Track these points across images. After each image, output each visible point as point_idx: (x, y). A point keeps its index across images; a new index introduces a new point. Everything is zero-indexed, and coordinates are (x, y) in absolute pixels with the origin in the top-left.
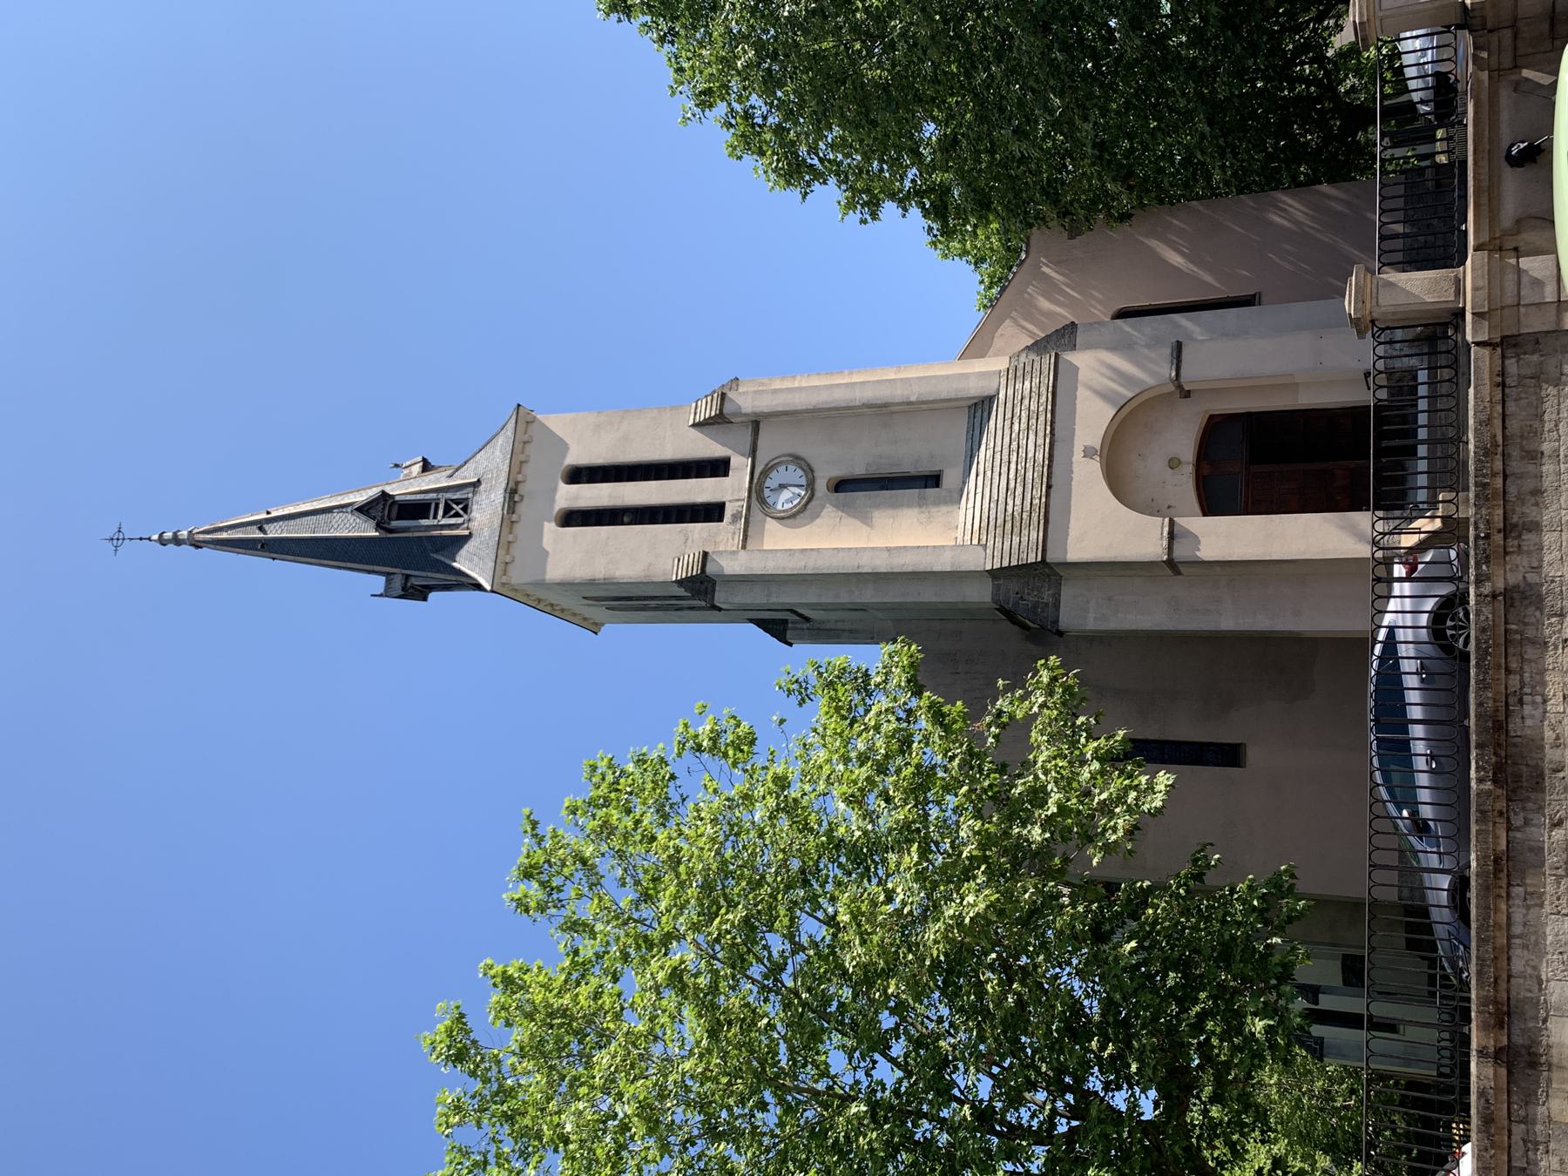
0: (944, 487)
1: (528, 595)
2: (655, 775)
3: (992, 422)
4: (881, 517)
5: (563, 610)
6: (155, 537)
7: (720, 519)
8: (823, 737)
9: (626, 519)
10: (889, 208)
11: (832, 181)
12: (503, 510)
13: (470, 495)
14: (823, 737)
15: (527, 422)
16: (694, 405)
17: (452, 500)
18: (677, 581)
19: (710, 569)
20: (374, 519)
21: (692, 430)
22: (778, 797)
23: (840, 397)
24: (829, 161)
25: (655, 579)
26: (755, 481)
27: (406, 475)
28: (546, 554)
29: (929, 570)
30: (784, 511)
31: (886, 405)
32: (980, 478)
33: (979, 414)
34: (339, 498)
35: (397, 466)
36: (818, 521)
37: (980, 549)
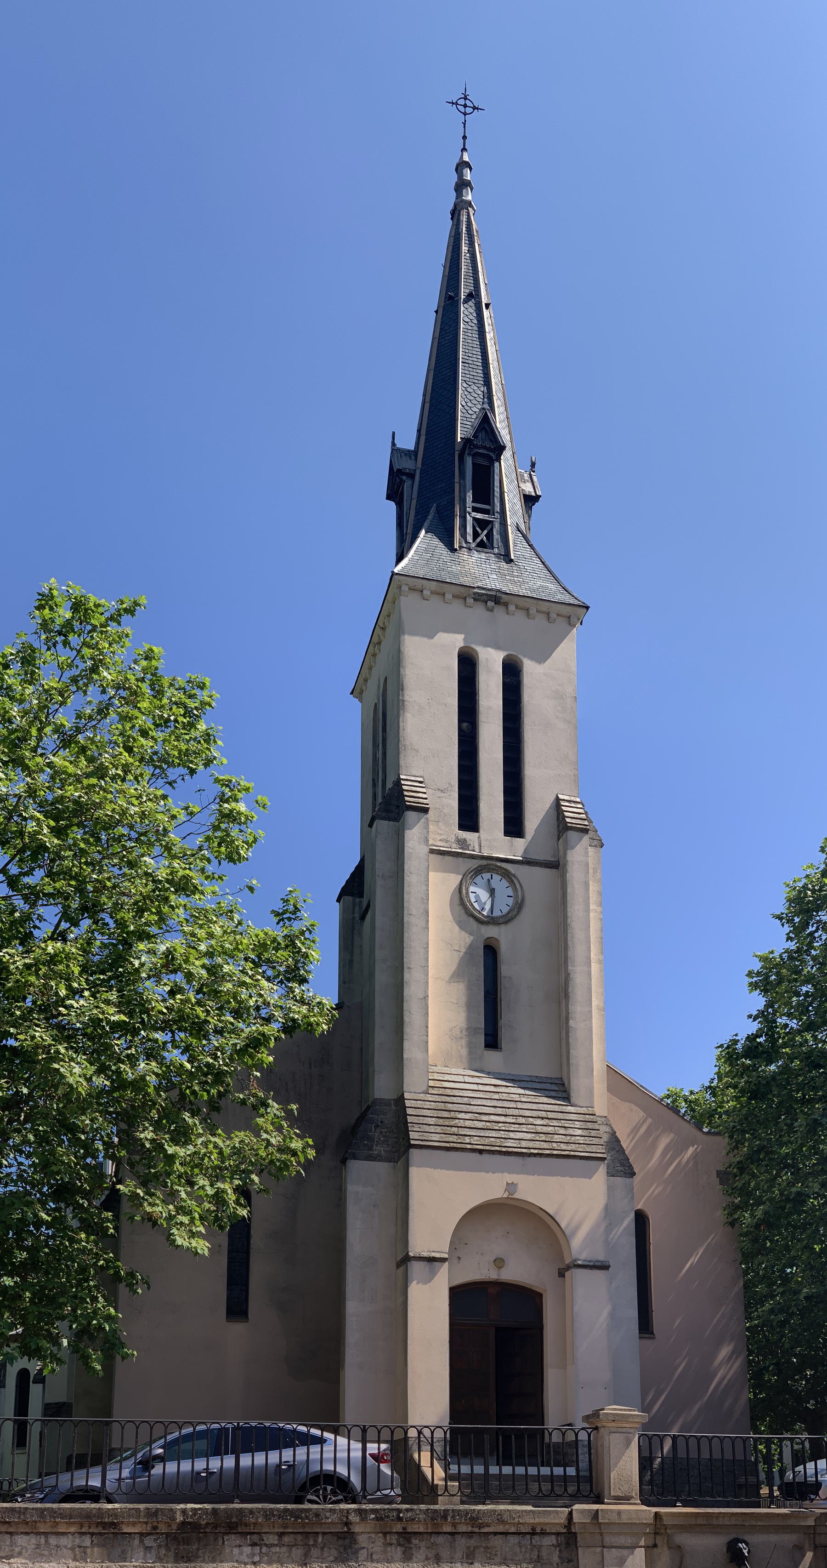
0: (485, 1052)
1: (389, 616)
2: (195, 753)
3: (545, 1100)
4: (459, 991)
5: (374, 655)
6: (466, 158)
7: (462, 827)
8: (234, 932)
9: (465, 725)
10: (758, 1001)
11: (792, 945)
12: (478, 587)
13: (496, 551)
14: (234, 932)
15: (569, 617)
16: (578, 800)
17: (492, 529)
18: (399, 779)
19: (410, 815)
20: (475, 436)
21: (553, 798)
22: (167, 881)
23: (577, 952)
24: (811, 943)
25: (401, 756)
26: (499, 864)
27: (522, 476)
28: (431, 637)
29: (405, 1037)
30: (467, 893)
31: (567, 996)
32: (492, 1089)
33: (554, 1087)
34: (500, 395)
35: (533, 465)
36: (457, 928)
37: (424, 1088)
